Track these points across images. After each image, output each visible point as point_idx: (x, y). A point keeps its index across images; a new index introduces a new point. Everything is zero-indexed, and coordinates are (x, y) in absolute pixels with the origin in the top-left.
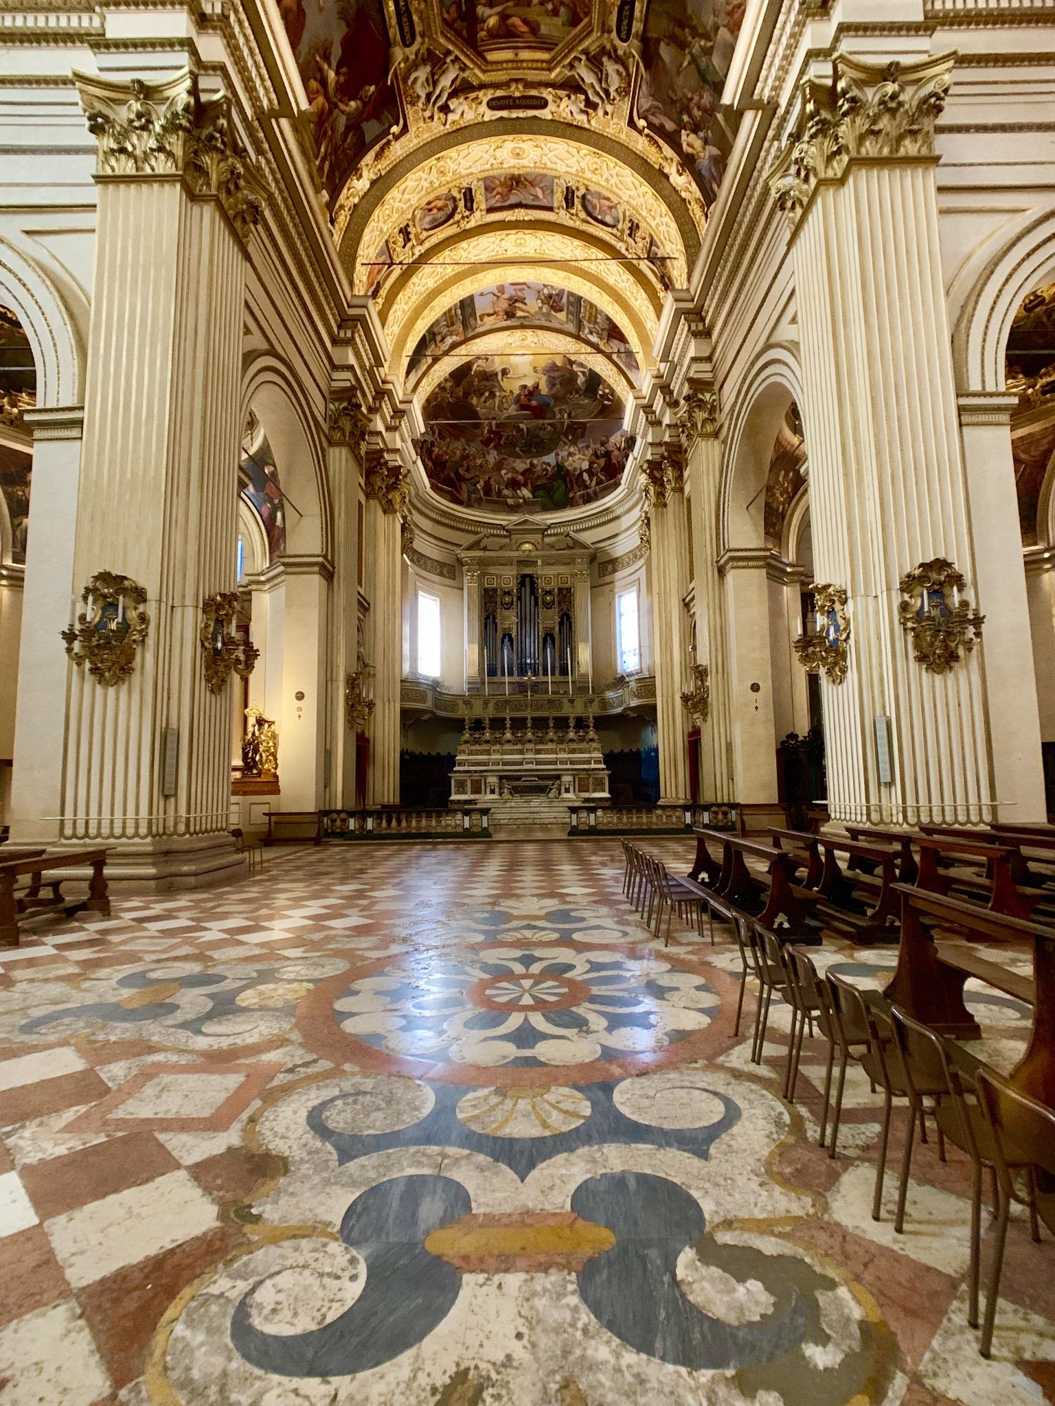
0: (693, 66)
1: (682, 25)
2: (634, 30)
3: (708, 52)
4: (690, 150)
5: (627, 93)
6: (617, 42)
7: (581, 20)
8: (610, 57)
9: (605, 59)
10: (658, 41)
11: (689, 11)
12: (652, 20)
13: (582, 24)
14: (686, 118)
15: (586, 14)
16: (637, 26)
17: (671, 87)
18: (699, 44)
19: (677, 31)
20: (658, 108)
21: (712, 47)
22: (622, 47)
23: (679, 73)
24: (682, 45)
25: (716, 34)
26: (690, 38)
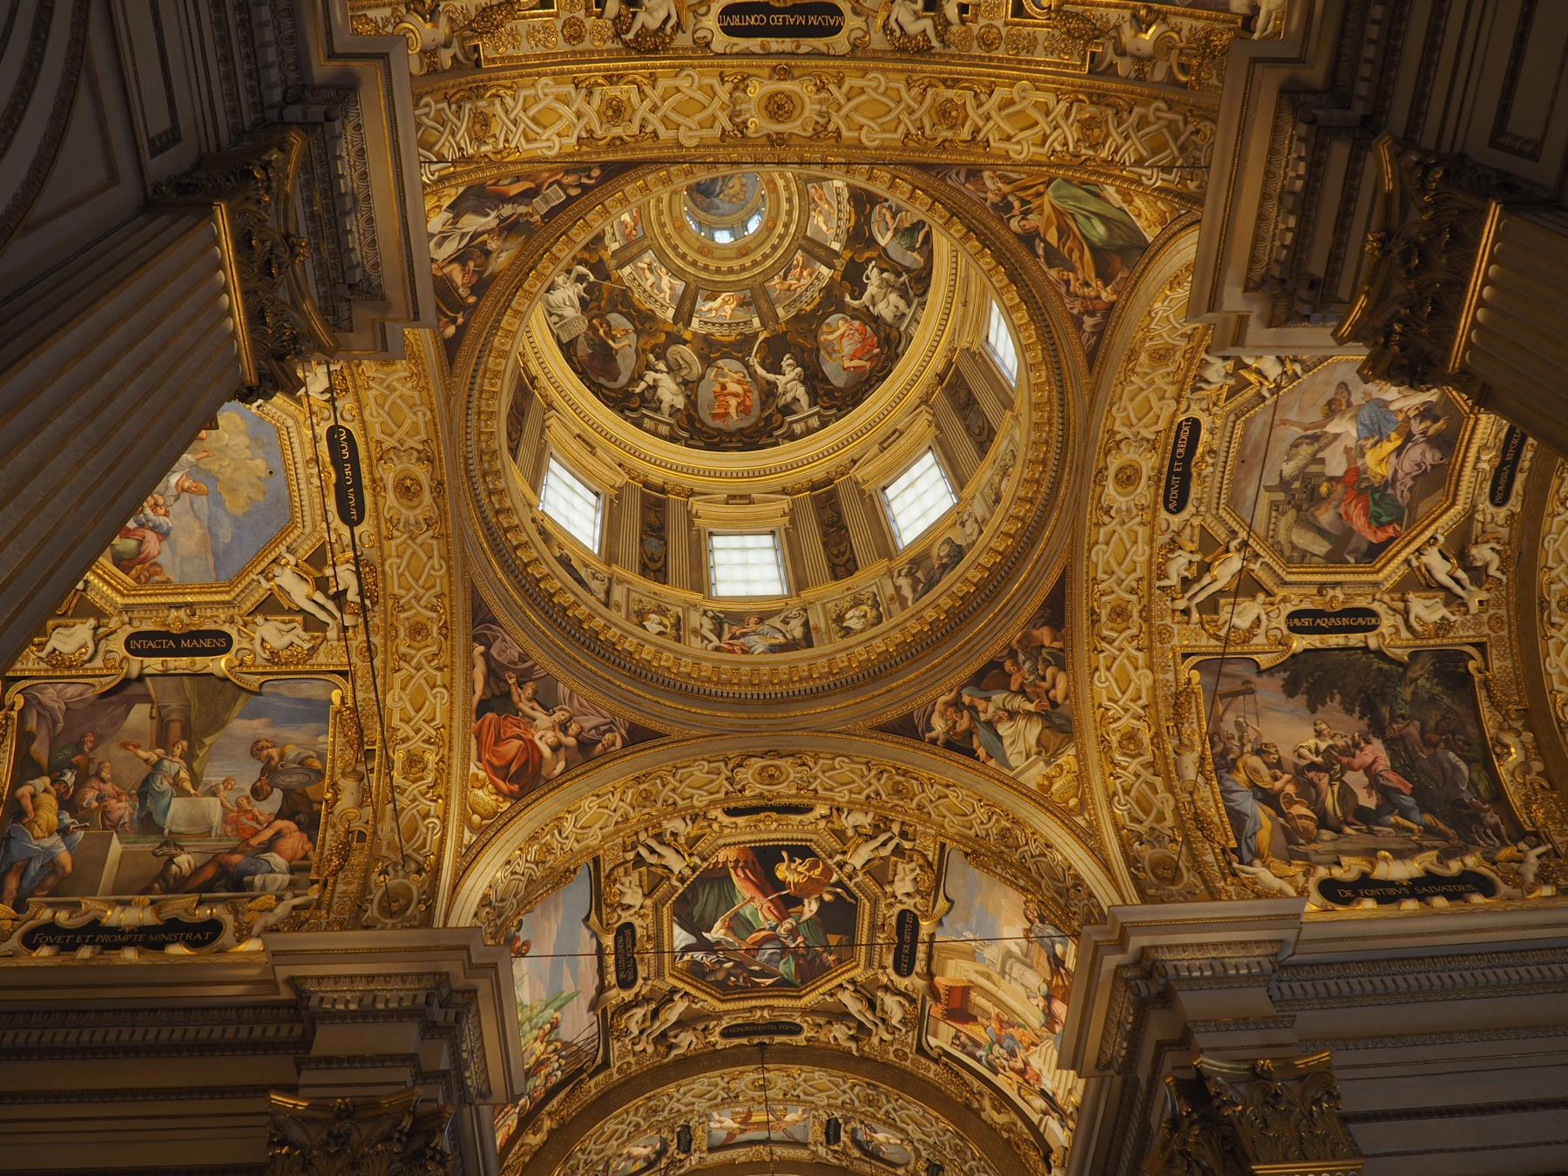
0: (146, 769)
1: (186, 733)
2: (148, 661)
3: (181, 792)
4: (27, 803)
5: (54, 667)
6: (122, 636)
7: (126, 571)
8: (96, 629)
9: (92, 622)
10: (146, 698)
11: (207, 741)
12: (168, 681)
13: (121, 574)
14: (69, 778)
15: (137, 579)
16: (154, 664)
17: (100, 739)
18: (174, 765)
19: (176, 729)
20: (55, 723)
21: (188, 794)
22: (117, 645)
23: (125, 746)
24: (162, 740)
25: (204, 795)
26: (178, 751)
